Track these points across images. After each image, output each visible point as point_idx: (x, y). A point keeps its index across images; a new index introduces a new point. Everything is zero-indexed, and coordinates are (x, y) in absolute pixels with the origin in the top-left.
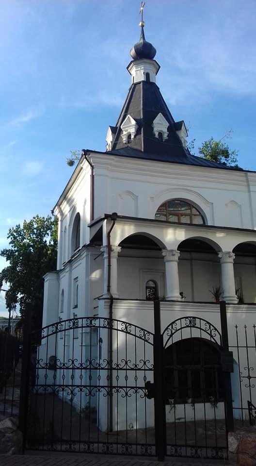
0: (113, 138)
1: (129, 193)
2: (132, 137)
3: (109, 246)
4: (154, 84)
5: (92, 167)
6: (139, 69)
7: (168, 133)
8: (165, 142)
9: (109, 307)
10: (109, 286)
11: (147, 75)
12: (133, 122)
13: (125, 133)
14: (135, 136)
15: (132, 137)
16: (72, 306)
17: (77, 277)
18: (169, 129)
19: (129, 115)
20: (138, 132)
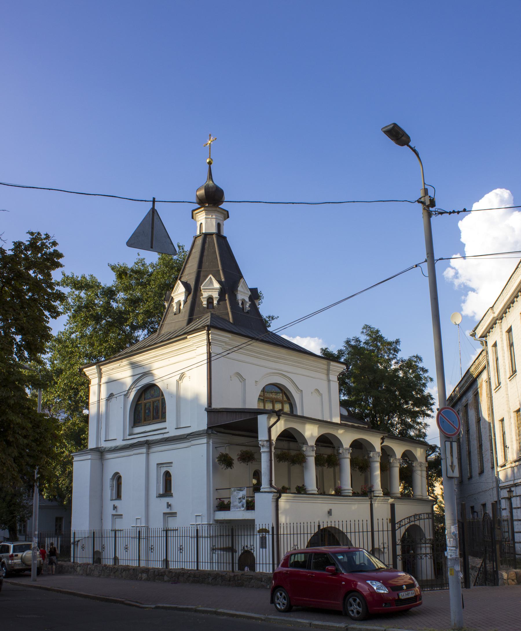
0: (187, 297)
1: (238, 375)
2: (215, 302)
3: (270, 440)
4: (225, 238)
5: (209, 344)
6: (210, 216)
7: (250, 303)
8: (248, 312)
9: (275, 500)
10: (271, 480)
11: (219, 226)
12: (217, 285)
13: (205, 294)
14: (218, 302)
15: (215, 302)
16: (153, 493)
17: (171, 463)
18: (250, 298)
19: (211, 276)
20: (222, 298)
